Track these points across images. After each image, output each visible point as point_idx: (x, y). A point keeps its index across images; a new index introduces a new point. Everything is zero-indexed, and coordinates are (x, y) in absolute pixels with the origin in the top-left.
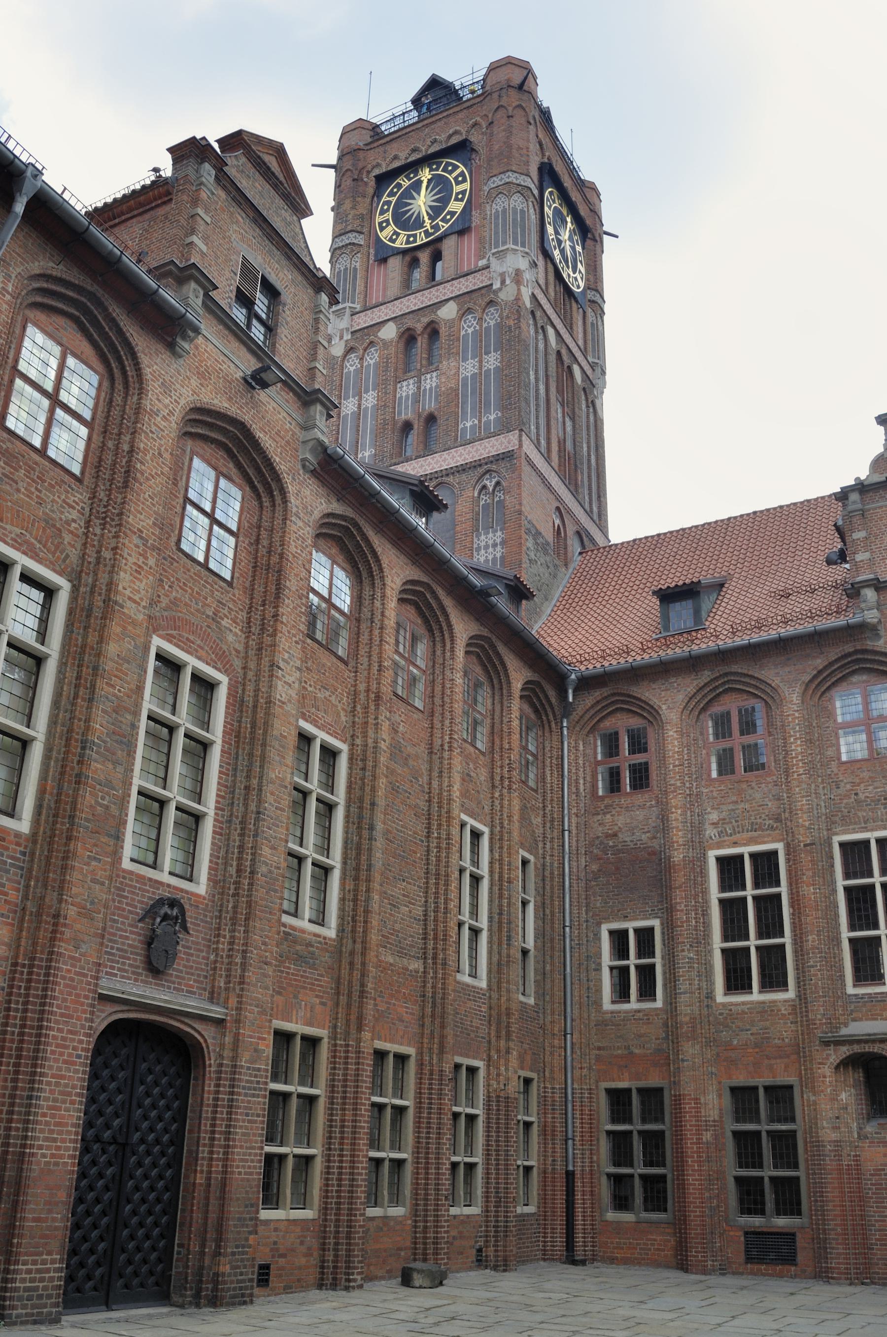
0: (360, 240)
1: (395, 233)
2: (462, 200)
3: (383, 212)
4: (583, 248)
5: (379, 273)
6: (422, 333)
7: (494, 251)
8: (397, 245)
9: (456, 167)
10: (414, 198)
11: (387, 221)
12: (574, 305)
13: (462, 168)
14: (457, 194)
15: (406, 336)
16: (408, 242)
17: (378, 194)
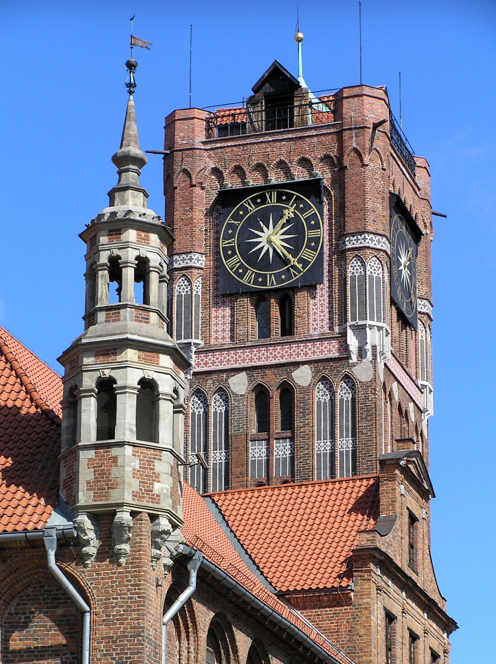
2: (315, 249)
8: (244, 281)
11: (232, 248)
14: (310, 240)
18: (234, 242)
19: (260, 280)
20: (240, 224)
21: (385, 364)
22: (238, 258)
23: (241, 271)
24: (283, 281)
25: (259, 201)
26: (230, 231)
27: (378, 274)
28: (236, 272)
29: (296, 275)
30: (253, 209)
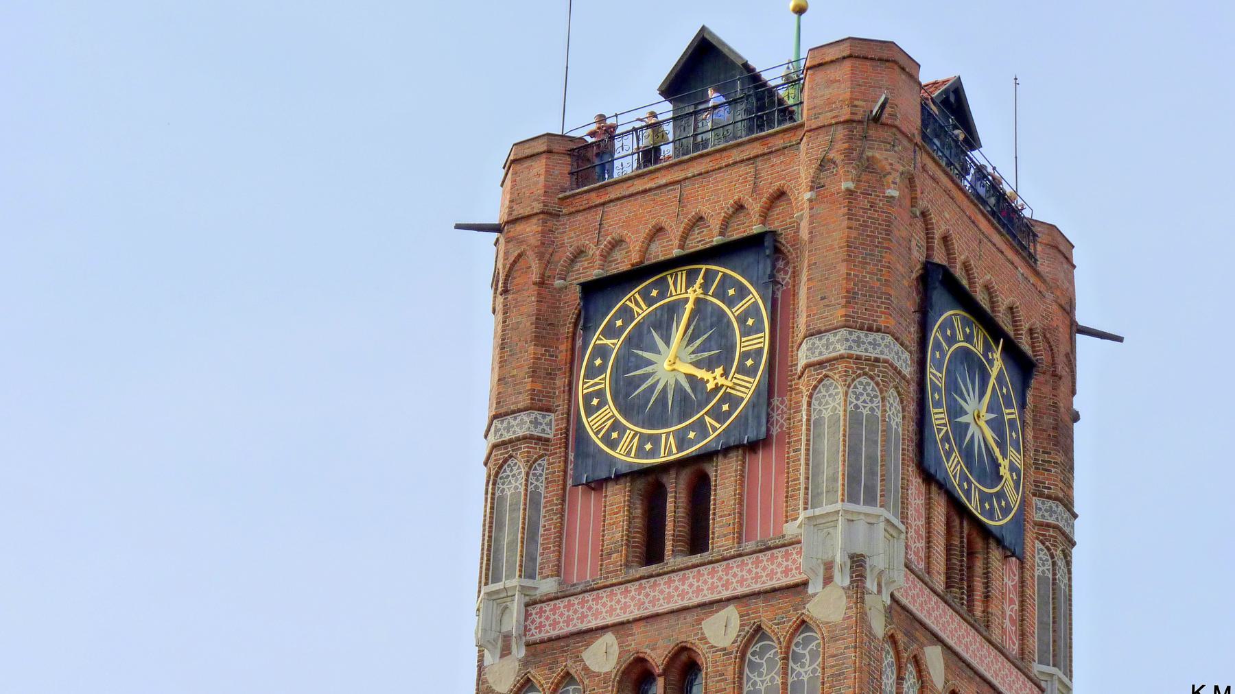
0: (550, 426)
1: (616, 426)
2: (752, 372)
3: (592, 372)
4: (1023, 405)
5: (586, 507)
6: (665, 673)
7: (810, 513)
8: (619, 454)
9: (742, 292)
10: (654, 349)
11: (600, 394)
12: (995, 554)
13: (754, 296)
14: (745, 355)
15: (637, 670)
16: (640, 452)
17: (585, 321)
18: (604, 382)
19: (648, 447)
20: (615, 344)
21: (892, 595)
22: (611, 409)
23: (615, 435)
24: (692, 443)
25: (654, 293)
26: (598, 362)
27: (872, 409)
28: (607, 440)
29: (715, 429)
30: (642, 311)
